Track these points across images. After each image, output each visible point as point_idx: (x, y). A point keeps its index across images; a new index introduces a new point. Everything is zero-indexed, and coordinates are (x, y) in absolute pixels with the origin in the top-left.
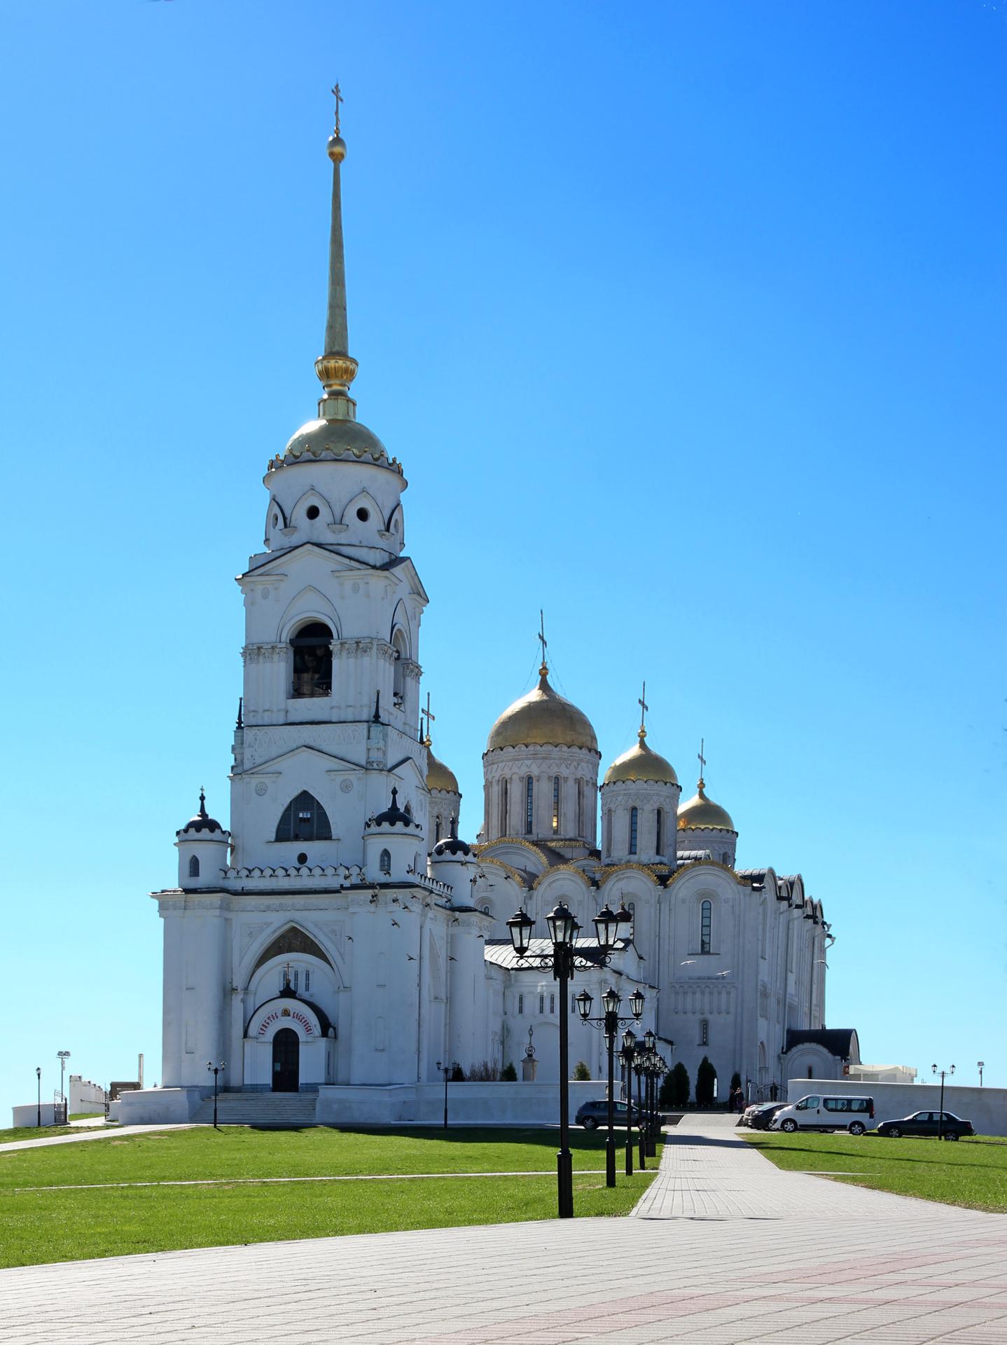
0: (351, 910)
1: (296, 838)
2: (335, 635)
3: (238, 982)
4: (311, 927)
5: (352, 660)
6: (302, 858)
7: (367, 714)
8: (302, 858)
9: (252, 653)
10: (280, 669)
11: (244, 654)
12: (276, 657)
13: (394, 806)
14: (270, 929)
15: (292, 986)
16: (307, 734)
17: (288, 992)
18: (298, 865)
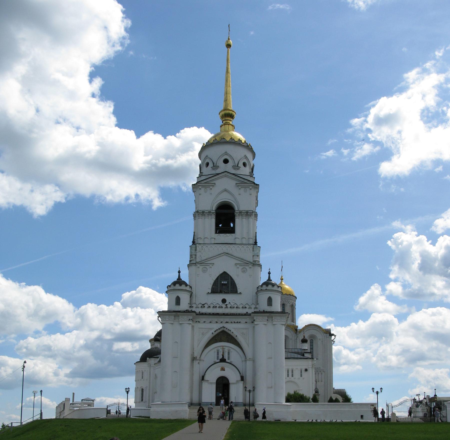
0: (255, 323)
1: (221, 292)
2: (236, 209)
3: (197, 354)
4: (232, 330)
5: (244, 220)
6: (224, 301)
7: (252, 242)
8: (224, 301)
9: (198, 214)
10: (211, 222)
11: (195, 216)
12: (210, 217)
13: (269, 279)
14: (213, 331)
15: (226, 357)
16: (225, 248)
17: (223, 360)
18: (221, 303)
